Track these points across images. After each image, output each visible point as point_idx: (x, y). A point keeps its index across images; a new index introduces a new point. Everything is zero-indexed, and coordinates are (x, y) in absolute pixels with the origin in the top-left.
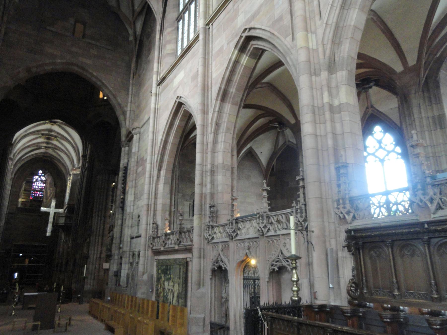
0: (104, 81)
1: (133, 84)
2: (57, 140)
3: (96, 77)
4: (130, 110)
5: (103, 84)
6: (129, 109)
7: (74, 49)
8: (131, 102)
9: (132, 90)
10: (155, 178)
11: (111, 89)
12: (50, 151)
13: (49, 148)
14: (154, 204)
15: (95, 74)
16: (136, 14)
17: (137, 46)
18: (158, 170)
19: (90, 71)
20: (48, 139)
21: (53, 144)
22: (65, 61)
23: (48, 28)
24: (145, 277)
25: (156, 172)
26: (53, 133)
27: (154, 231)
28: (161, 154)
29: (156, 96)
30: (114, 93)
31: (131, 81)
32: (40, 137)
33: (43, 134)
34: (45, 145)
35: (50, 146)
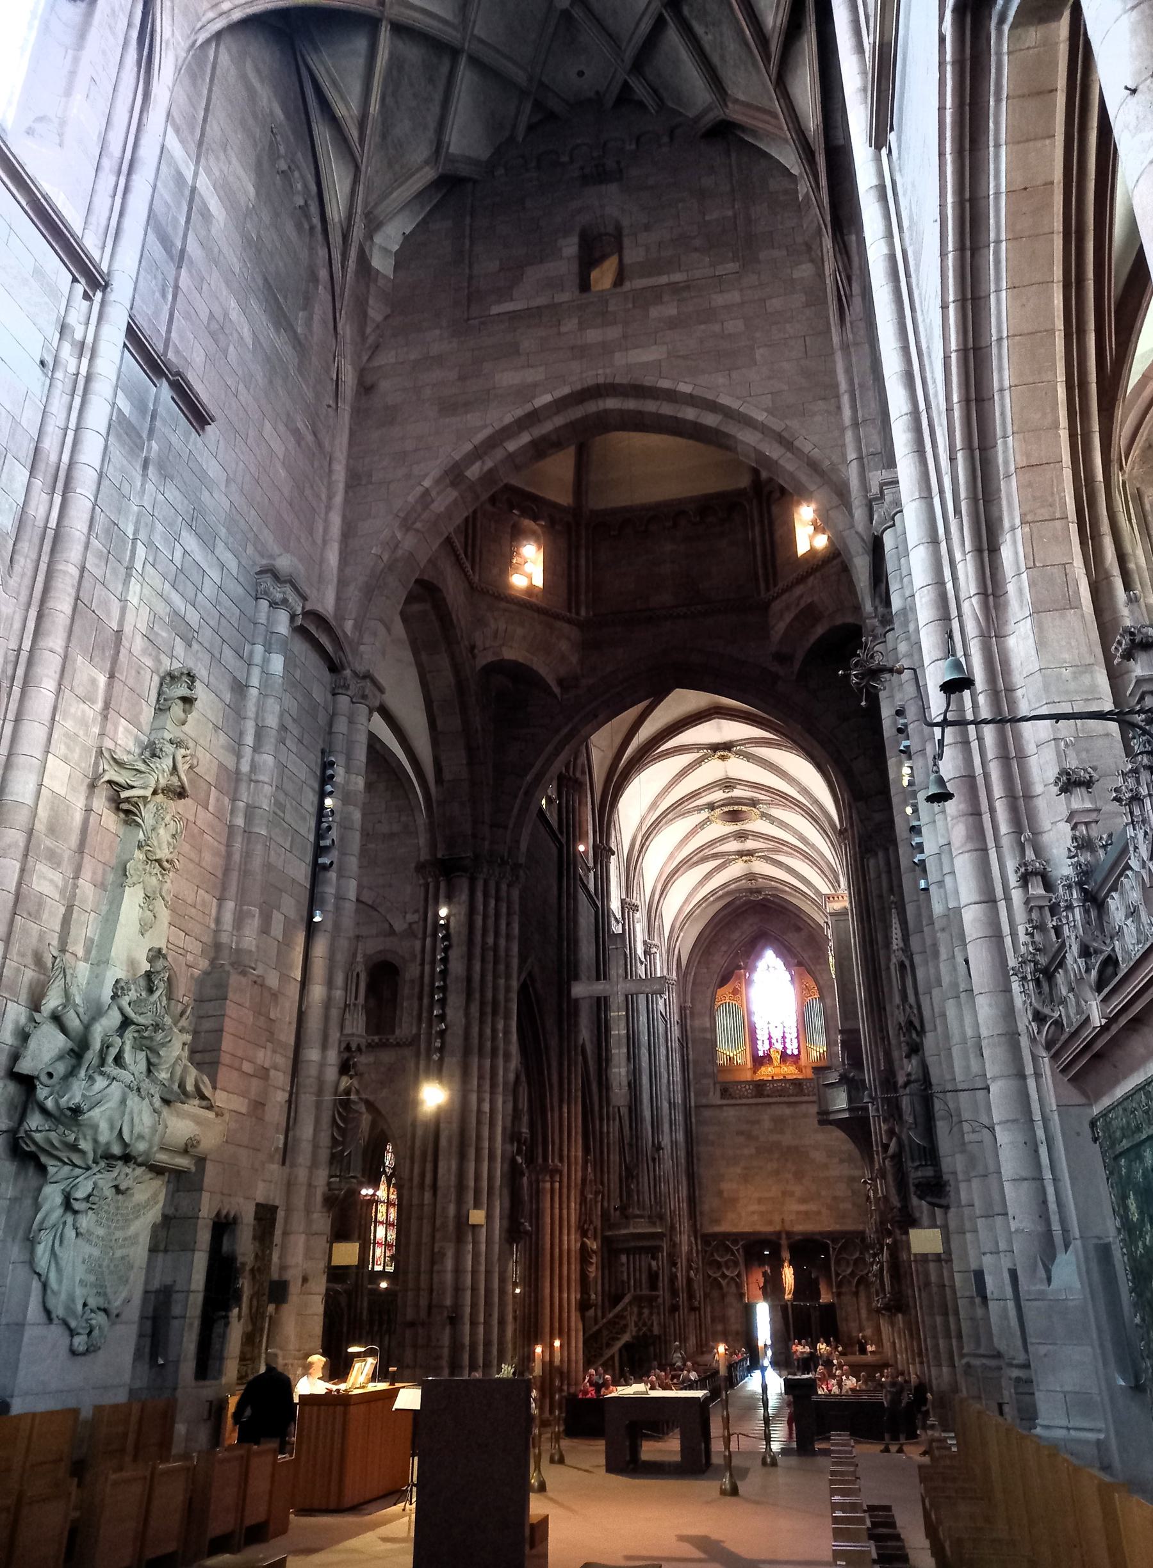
0: (725, 400)
1: (845, 348)
2: (764, 815)
3: (692, 400)
4: (860, 458)
5: (728, 413)
6: (852, 455)
7: (593, 336)
8: (856, 424)
9: (848, 370)
10: (971, 606)
11: (761, 417)
12: (761, 867)
13: (750, 853)
14: (1005, 758)
15: (685, 388)
16: (775, 46)
17: (823, 182)
18: (978, 550)
19: (665, 384)
20: (734, 817)
21: (758, 836)
22: (566, 390)
23: (495, 310)
24: (1068, 1272)
25: (967, 570)
26: (737, 793)
27: (1040, 927)
28: (969, 447)
29: (883, 197)
30: (777, 425)
31: (836, 339)
32: (708, 821)
33: (711, 806)
34: (734, 846)
35: (750, 844)
